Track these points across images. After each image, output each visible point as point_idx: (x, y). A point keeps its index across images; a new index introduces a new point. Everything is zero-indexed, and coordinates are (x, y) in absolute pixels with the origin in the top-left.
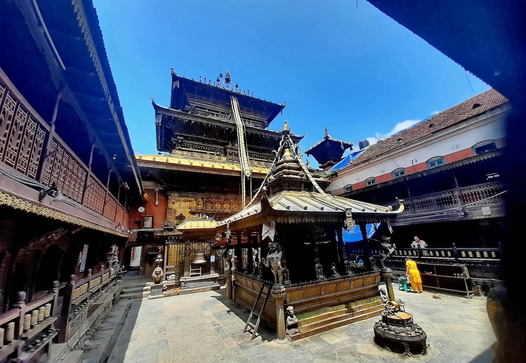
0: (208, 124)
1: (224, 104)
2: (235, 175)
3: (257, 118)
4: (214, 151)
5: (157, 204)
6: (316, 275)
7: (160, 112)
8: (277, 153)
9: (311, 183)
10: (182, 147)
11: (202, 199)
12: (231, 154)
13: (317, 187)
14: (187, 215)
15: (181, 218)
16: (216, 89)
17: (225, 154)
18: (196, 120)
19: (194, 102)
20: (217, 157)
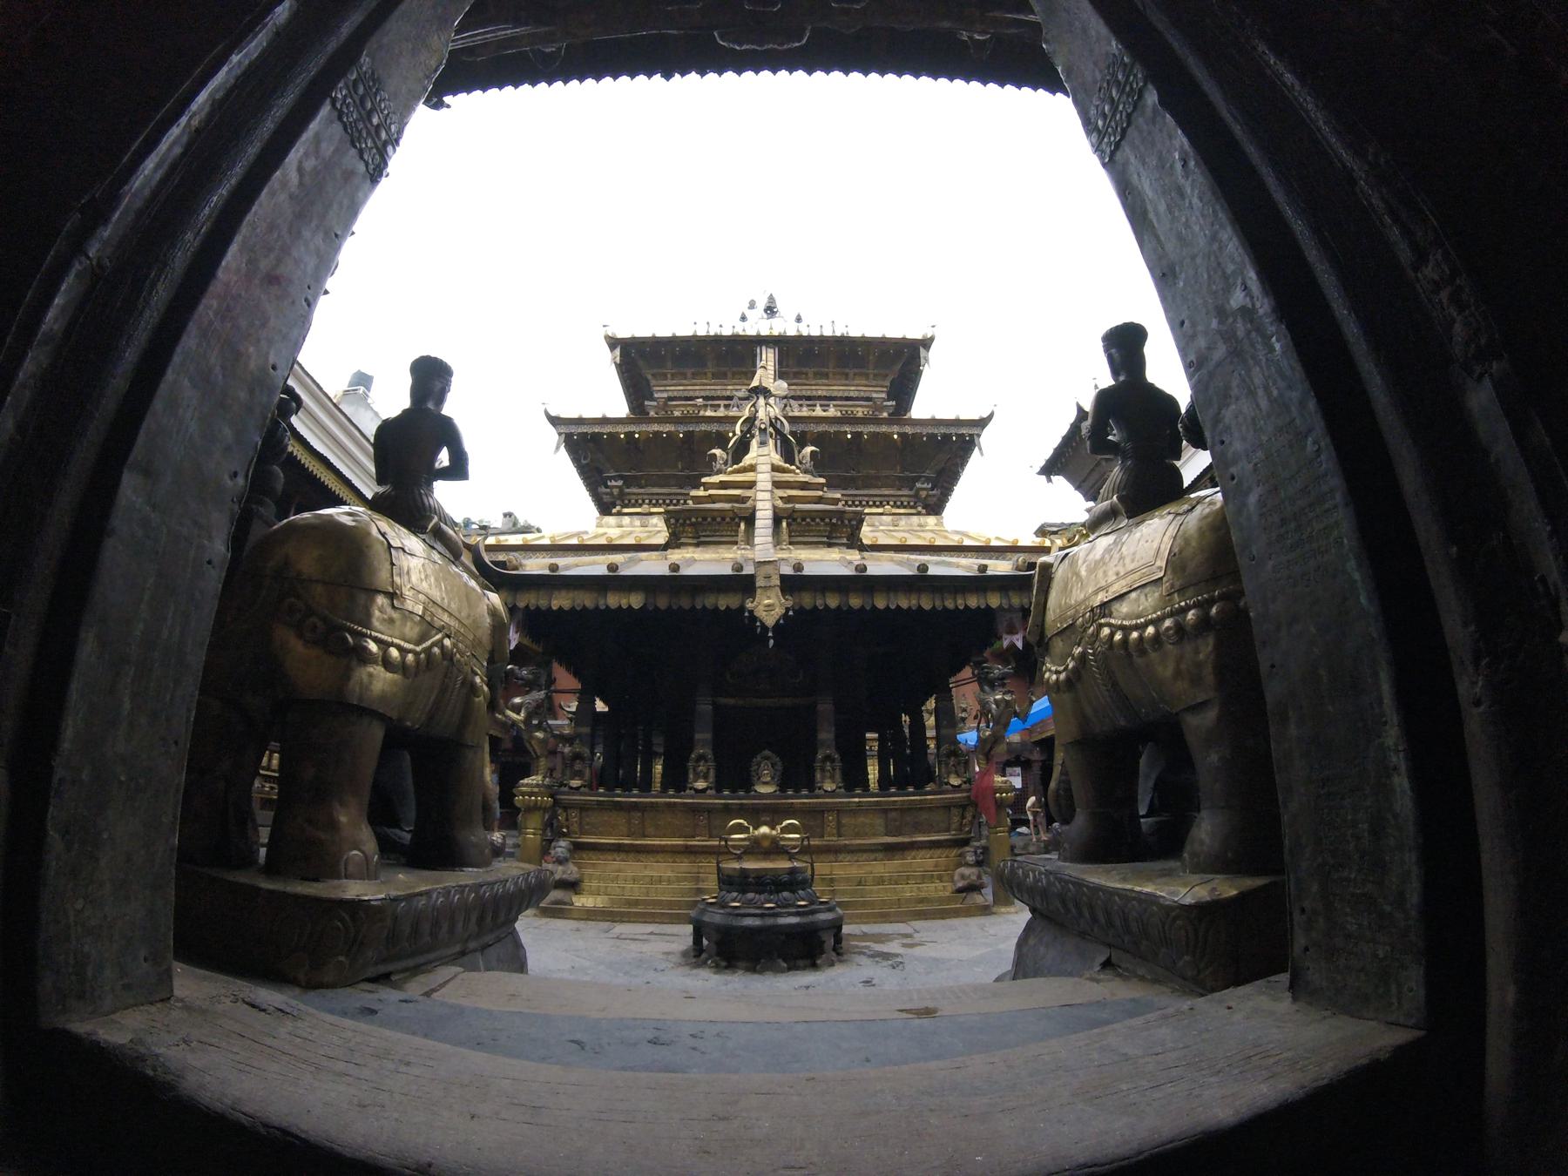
3: (852, 391)
7: (564, 429)
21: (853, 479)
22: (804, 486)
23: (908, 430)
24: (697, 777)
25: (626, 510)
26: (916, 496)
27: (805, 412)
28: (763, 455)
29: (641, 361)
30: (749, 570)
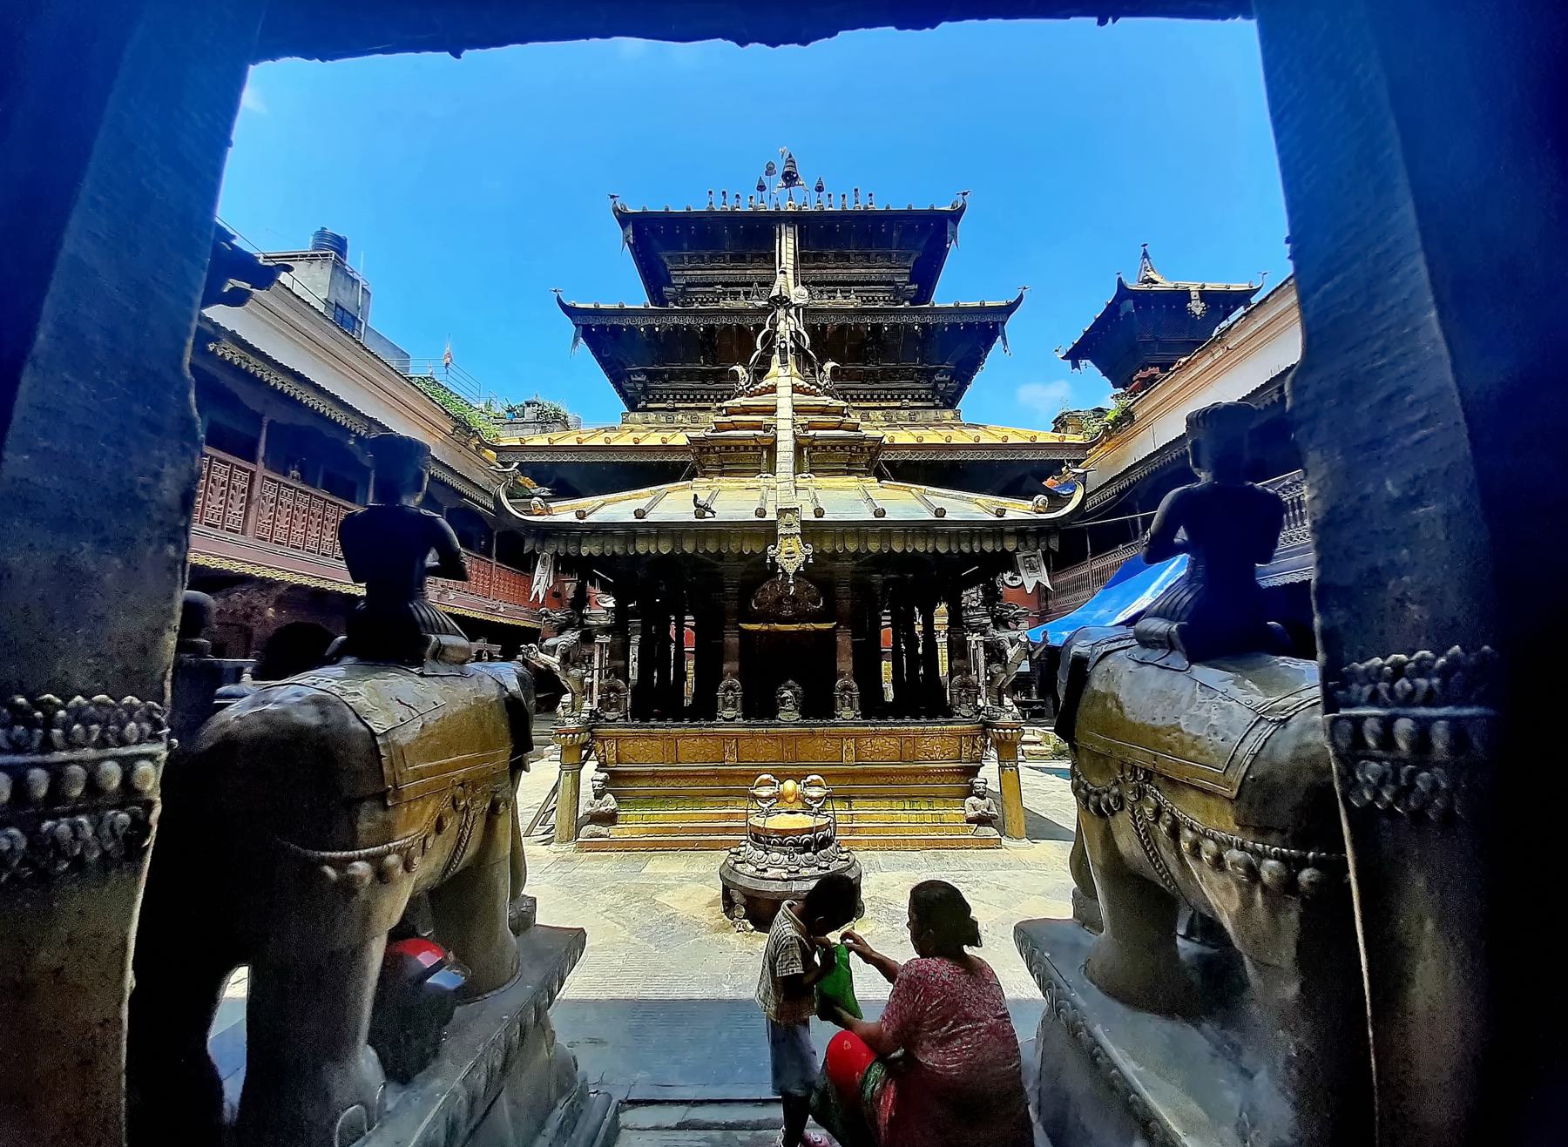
3: (874, 273)
7: (580, 320)
10: (650, 401)
22: (824, 410)
23: (929, 320)
24: (726, 705)
26: (935, 388)
27: (825, 303)
28: (783, 375)
29: (655, 238)
30: (771, 516)
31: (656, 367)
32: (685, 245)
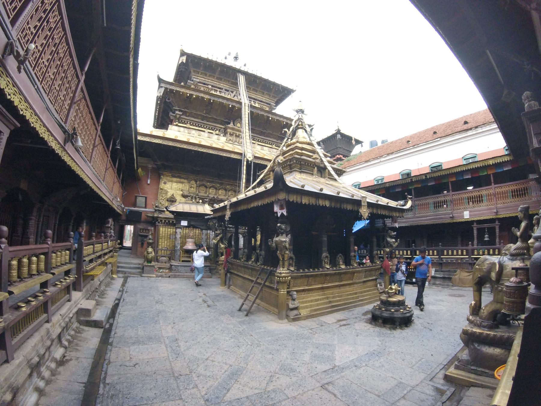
0: (210, 99)
1: (229, 81)
2: (234, 157)
4: (213, 130)
5: (149, 183)
6: (322, 263)
7: (162, 85)
8: (289, 132)
9: (325, 168)
11: (196, 181)
12: (231, 135)
13: (333, 173)
14: (179, 198)
15: (172, 200)
16: (223, 66)
17: (225, 134)
18: (198, 94)
19: (197, 78)
20: (217, 136)
21: (264, 133)
25: (180, 124)
31: (186, 110)
32: (201, 68)
